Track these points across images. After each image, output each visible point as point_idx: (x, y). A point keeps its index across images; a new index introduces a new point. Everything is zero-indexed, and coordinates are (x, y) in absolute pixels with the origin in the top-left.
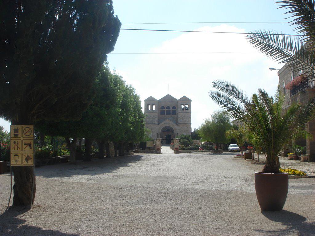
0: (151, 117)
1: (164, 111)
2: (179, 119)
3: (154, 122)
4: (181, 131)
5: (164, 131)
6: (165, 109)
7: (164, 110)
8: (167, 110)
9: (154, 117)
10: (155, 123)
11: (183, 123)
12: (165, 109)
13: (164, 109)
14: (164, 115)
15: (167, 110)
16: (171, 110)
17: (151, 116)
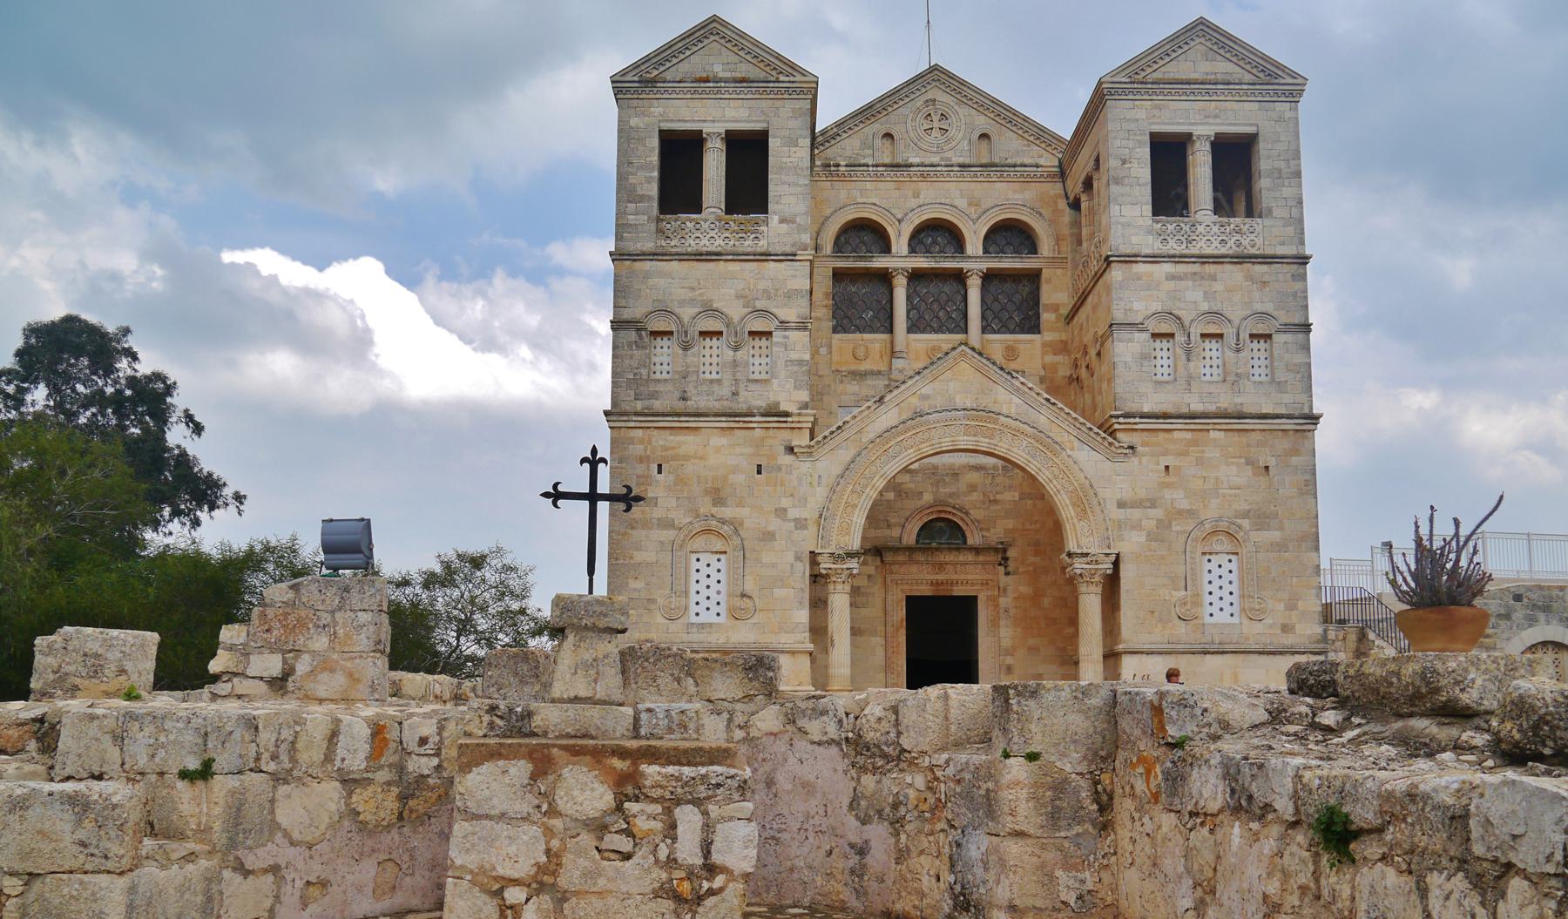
1: (885, 277)
2: (1126, 349)
3: (754, 398)
4: (1165, 525)
6: (900, 258)
7: (880, 262)
8: (922, 262)
9: (758, 326)
11: (1197, 407)
12: (900, 258)
13: (886, 249)
14: (877, 340)
16: (975, 259)
17: (710, 310)
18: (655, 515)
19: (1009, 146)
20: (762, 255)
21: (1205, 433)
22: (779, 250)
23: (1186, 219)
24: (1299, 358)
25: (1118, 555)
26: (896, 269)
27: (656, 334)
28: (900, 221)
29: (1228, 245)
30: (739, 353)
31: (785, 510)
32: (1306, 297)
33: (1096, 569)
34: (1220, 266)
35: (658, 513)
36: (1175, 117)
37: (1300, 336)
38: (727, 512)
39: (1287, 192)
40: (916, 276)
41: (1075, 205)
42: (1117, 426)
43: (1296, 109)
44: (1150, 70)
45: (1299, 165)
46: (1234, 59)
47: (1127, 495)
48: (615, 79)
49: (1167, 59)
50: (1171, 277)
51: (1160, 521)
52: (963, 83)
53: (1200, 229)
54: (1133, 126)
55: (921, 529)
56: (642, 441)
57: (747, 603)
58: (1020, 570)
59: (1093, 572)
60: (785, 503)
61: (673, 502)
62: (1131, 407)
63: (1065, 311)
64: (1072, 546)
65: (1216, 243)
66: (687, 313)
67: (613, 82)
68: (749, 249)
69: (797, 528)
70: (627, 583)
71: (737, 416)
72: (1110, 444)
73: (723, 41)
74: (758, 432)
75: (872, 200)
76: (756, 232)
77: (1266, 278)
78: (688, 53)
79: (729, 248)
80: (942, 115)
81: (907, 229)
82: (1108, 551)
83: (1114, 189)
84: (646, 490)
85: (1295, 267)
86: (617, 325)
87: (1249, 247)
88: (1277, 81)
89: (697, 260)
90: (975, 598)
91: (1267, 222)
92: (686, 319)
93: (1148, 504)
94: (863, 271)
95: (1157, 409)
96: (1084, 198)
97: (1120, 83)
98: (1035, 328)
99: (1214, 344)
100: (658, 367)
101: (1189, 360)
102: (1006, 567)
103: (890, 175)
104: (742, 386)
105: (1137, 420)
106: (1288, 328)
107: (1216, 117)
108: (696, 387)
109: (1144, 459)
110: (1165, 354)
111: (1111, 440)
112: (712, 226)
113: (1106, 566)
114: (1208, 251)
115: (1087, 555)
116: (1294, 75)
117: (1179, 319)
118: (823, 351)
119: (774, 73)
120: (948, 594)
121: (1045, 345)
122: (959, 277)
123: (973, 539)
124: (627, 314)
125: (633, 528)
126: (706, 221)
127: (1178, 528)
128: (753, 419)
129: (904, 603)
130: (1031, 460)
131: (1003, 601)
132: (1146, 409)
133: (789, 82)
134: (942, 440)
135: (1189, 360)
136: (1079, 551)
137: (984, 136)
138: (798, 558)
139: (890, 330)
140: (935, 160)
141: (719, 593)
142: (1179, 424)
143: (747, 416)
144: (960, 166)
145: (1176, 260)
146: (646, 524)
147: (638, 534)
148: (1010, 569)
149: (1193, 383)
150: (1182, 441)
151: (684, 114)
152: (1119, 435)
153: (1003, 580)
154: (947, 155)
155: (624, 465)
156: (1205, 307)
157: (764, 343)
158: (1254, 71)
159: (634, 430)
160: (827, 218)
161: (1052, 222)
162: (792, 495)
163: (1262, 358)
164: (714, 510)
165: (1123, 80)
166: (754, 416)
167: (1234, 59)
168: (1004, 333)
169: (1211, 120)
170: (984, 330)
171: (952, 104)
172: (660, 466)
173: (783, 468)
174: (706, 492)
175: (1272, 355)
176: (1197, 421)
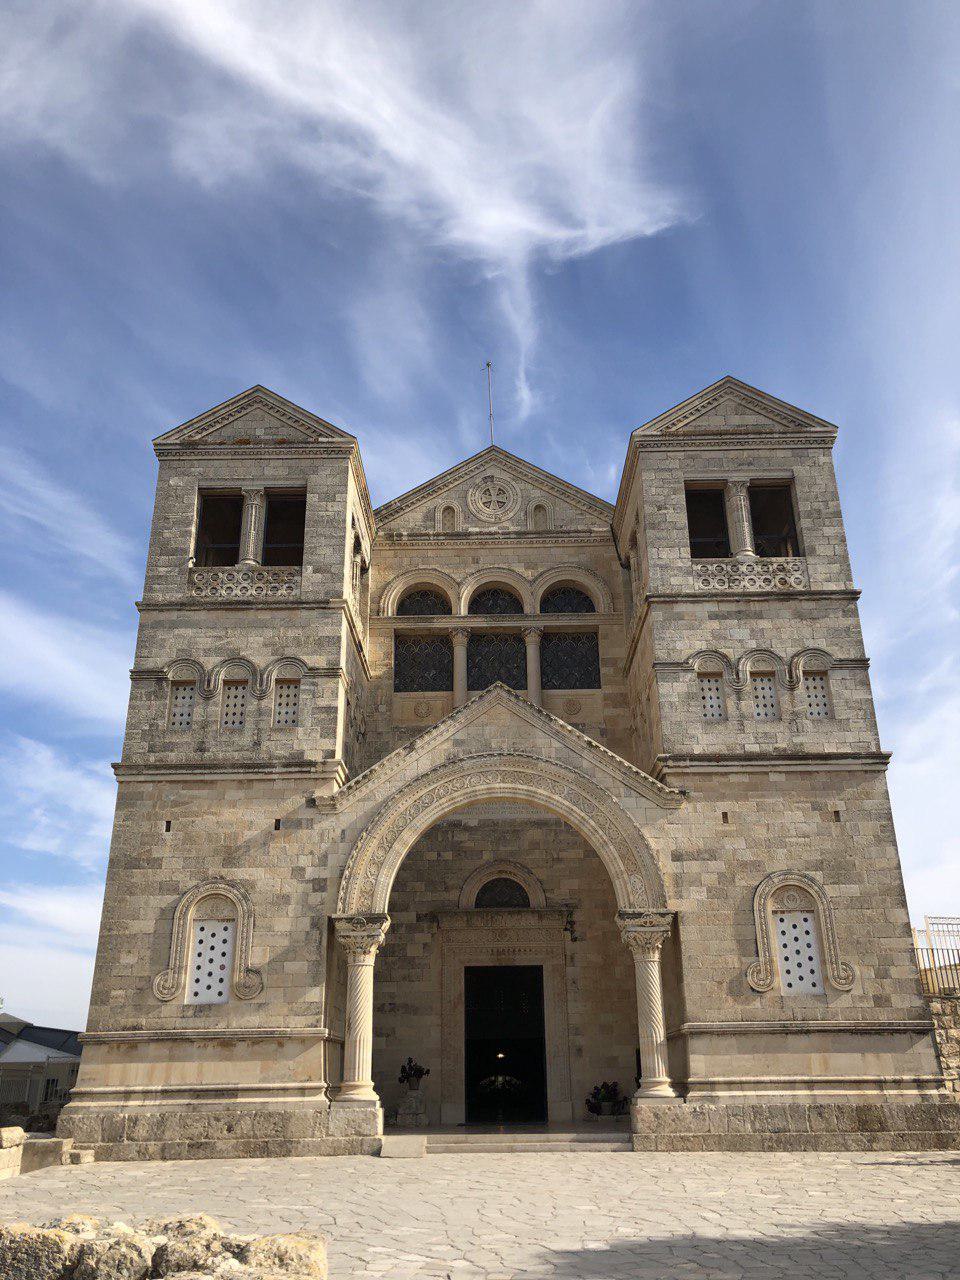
0: (239, 674)
1: (445, 640)
2: (672, 691)
3: (277, 747)
5: (433, 917)
7: (440, 623)
8: (480, 622)
10: (298, 764)
11: (755, 748)
14: (436, 698)
15: (480, 622)
16: (533, 621)
18: (158, 879)
19: (563, 514)
20: (292, 603)
21: (765, 776)
22: (311, 597)
23: (727, 560)
24: (860, 695)
25: (676, 915)
26: (456, 629)
27: (176, 684)
28: (459, 584)
29: (773, 584)
30: (264, 703)
31: (303, 869)
32: (860, 632)
33: (653, 932)
34: (765, 604)
35: (162, 875)
36: (710, 465)
37: (859, 674)
38: (240, 874)
39: (828, 531)
40: (475, 638)
41: (626, 566)
42: (666, 770)
43: (830, 455)
44: (681, 424)
45: (838, 506)
46: (763, 412)
47: (685, 846)
48: (157, 441)
49: (698, 414)
50: (713, 616)
51: (721, 875)
52: (519, 461)
53: (743, 568)
54: (666, 475)
55: (484, 890)
56: (151, 796)
57: (254, 979)
58: (588, 935)
59: (648, 936)
60: (304, 861)
61: (178, 864)
62: (684, 749)
63: (621, 665)
64: (622, 904)
65: (760, 582)
66: (210, 662)
67: (155, 445)
68: (282, 598)
69: (315, 890)
70: (119, 959)
71: (253, 769)
72: (660, 789)
73: (265, 408)
74: (279, 785)
75: (434, 566)
76: (290, 581)
77: (815, 614)
78: (231, 419)
79: (262, 598)
80: (500, 489)
81: (466, 593)
82: (662, 910)
83: (650, 533)
84: (149, 851)
85: (845, 602)
86: (137, 676)
87: (793, 584)
88: (805, 429)
89: (227, 610)
90: (539, 969)
91: (810, 560)
92: (208, 667)
93: (707, 856)
94: (427, 633)
95: (710, 750)
96: (632, 554)
97: (652, 436)
98: (594, 682)
99: (766, 684)
100: (178, 717)
101: (739, 699)
102: (572, 932)
103: (450, 544)
104: (264, 736)
105: (688, 763)
106: (842, 664)
107: (750, 464)
108: (215, 738)
109: (699, 805)
110: (713, 694)
111: (659, 785)
112: (245, 577)
113: (663, 929)
114: (752, 589)
115: (640, 915)
116: (823, 423)
117: (725, 656)
118: (382, 708)
119: (314, 435)
120: (510, 964)
121: (606, 698)
122: (518, 638)
123: (537, 899)
124: (150, 664)
125: (131, 894)
126: (238, 572)
127: (743, 883)
128: (274, 770)
129: (463, 975)
130: (574, 808)
131: (570, 969)
132: (697, 751)
133: (328, 442)
134: (477, 788)
135: (739, 699)
136: (630, 911)
137: (539, 508)
138: (315, 925)
139: (450, 688)
140: (493, 529)
141: (222, 967)
142: (735, 767)
143: (268, 767)
144: (516, 533)
145: (719, 599)
146: (147, 889)
147: (138, 900)
148: (577, 934)
149: (746, 722)
150: (739, 784)
151: (225, 473)
152: (669, 779)
153: (570, 946)
154: (504, 524)
155: (128, 823)
156: (753, 644)
157: (292, 691)
158: (784, 422)
159: (147, 785)
160: (389, 583)
161: (606, 583)
162: (311, 853)
163: (820, 696)
164: (224, 872)
165: (655, 433)
166: (274, 767)
167: (763, 412)
168: (564, 688)
169: (745, 467)
170: (544, 686)
171: (509, 480)
172: (168, 823)
173: (304, 822)
174: (216, 852)
175: (830, 693)
176: (753, 763)
